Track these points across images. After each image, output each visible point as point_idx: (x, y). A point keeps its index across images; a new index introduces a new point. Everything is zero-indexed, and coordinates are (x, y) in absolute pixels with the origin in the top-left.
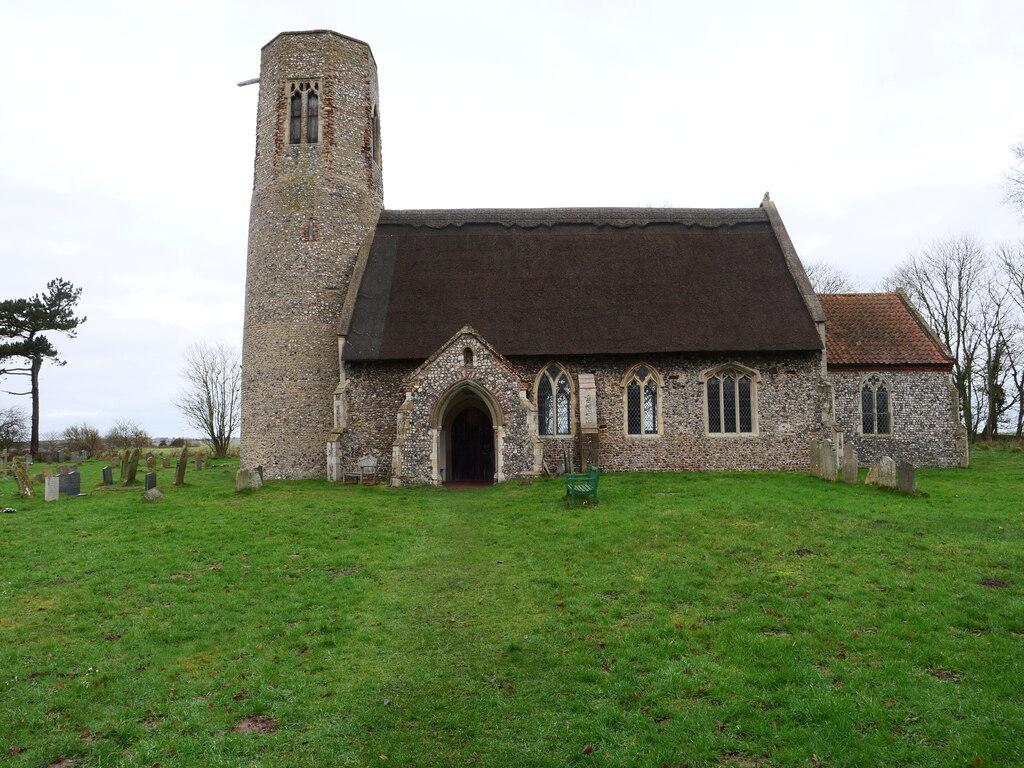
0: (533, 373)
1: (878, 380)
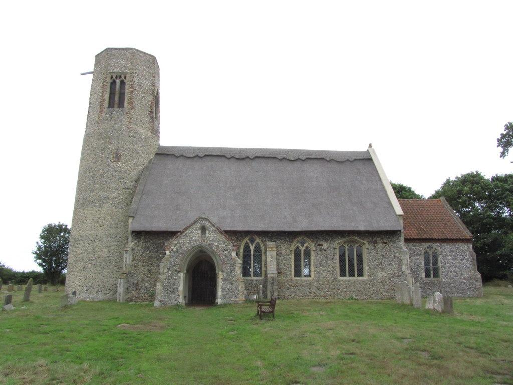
0: (241, 241)
1: (432, 247)
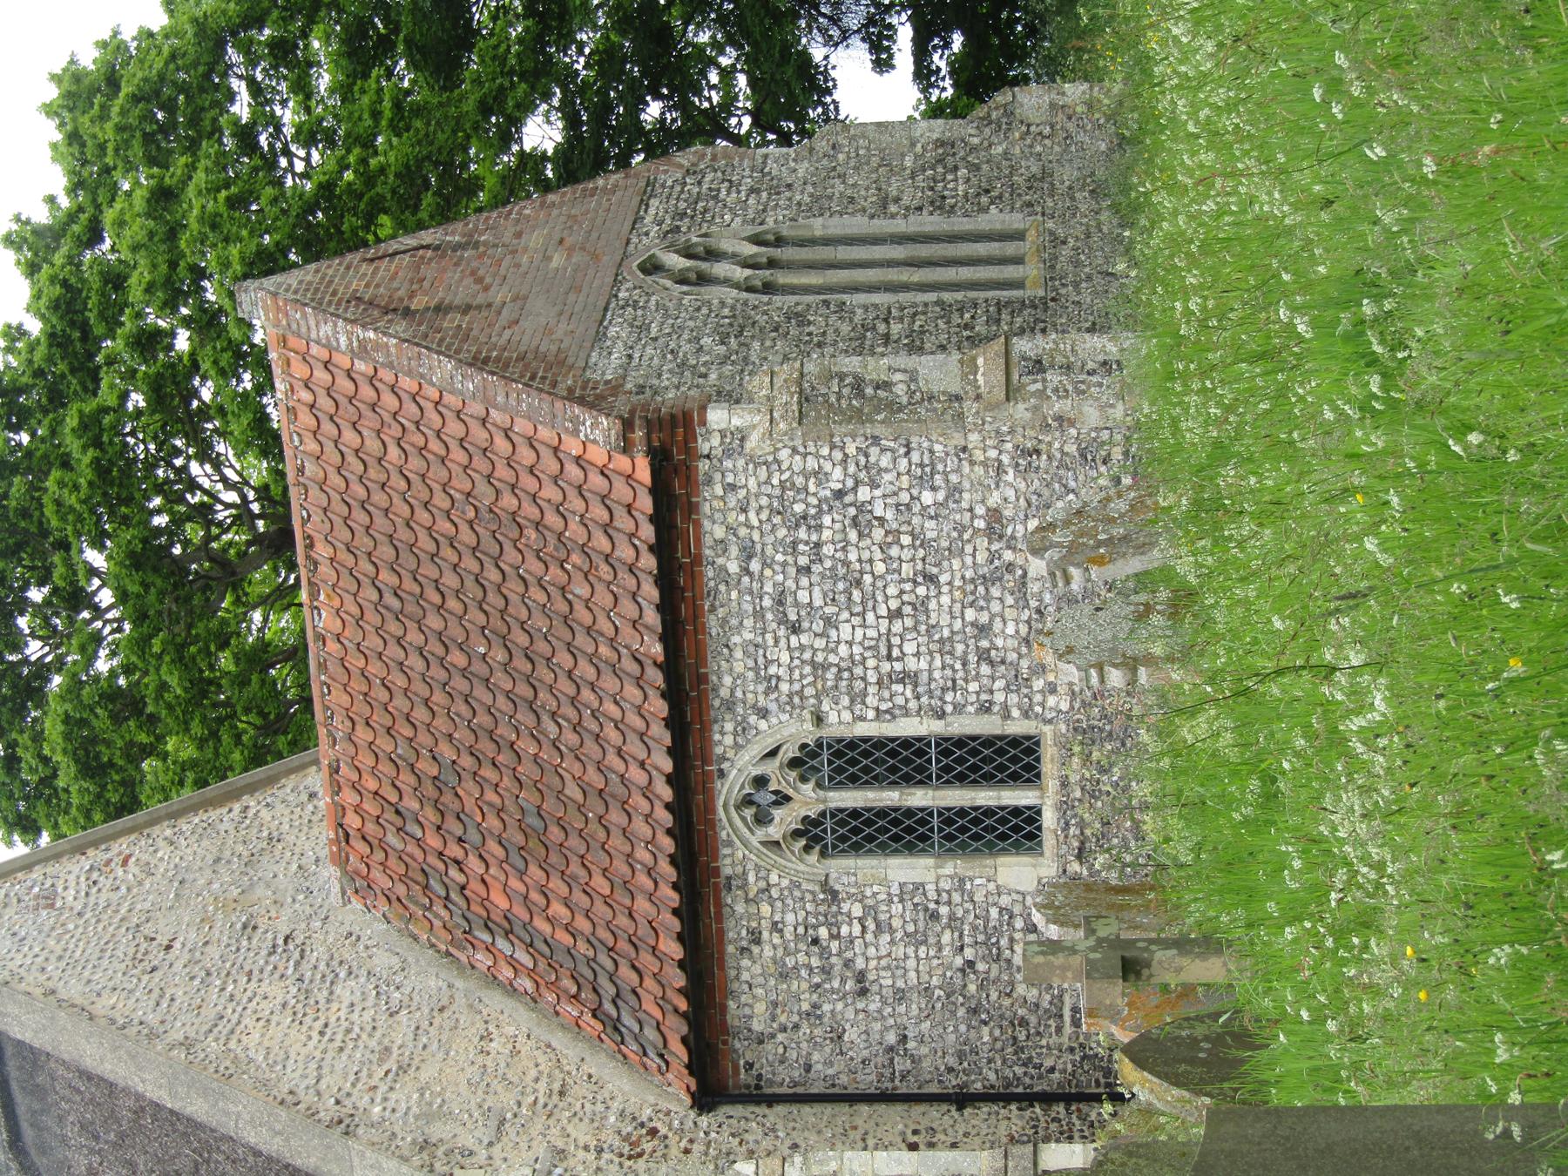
1: (760, 782)
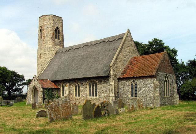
1: (135, 82)
